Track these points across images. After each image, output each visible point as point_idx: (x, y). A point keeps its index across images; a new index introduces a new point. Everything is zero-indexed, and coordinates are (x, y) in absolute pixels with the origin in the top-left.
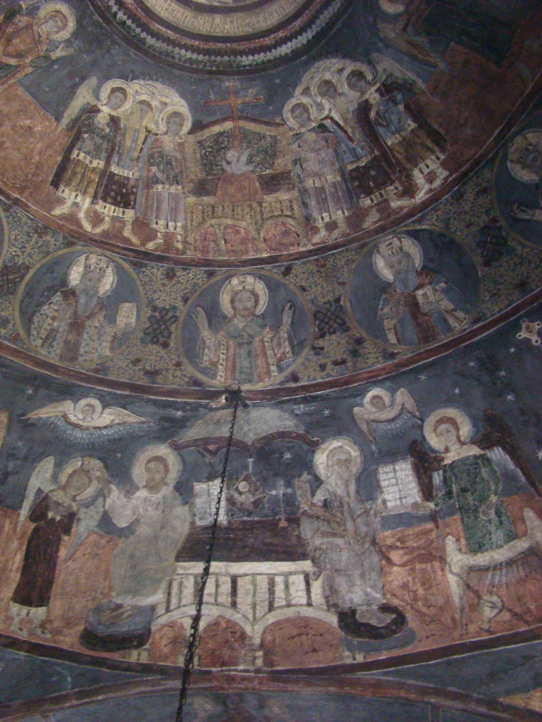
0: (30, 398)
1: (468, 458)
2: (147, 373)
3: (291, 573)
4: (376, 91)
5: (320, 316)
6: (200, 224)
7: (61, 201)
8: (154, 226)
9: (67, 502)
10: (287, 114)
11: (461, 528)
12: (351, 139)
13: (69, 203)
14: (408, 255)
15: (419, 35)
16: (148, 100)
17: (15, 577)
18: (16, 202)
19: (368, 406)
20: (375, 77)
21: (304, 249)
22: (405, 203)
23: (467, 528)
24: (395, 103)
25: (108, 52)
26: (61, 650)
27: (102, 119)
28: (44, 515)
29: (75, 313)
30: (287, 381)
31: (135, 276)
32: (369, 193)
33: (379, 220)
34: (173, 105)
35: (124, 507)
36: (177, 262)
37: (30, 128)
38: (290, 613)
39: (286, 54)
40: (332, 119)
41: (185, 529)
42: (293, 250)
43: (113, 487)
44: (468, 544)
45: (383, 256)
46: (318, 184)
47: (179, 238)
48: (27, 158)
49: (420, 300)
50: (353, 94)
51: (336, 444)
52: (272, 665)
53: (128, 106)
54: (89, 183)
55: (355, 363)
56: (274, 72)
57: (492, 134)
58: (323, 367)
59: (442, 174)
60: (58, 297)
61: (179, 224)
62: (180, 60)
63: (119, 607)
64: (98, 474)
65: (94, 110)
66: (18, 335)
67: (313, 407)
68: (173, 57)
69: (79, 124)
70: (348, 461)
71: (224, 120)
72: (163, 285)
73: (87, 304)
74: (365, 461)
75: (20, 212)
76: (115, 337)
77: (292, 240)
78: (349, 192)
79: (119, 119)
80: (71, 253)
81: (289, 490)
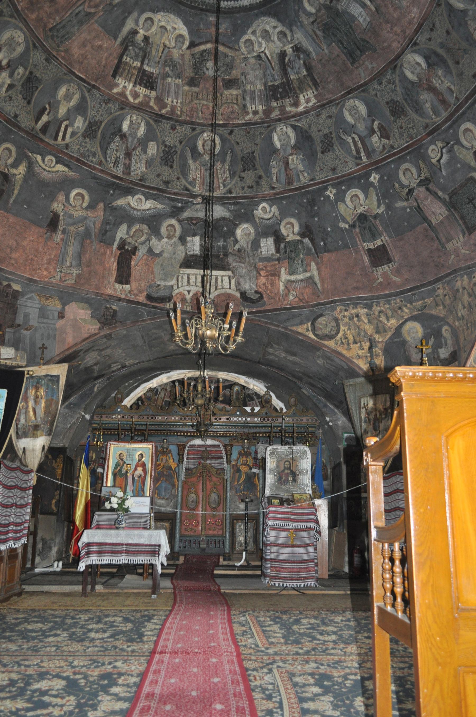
0: (112, 195)
1: (295, 240)
2: (164, 182)
3: (224, 276)
4: (291, 47)
5: (244, 159)
6: (190, 102)
7: (117, 85)
9: (133, 242)
10: (242, 45)
11: (287, 265)
12: (273, 68)
13: (121, 86)
14: (289, 137)
15: (319, 30)
16: (165, 25)
17: (115, 273)
18: (94, 86)
19: (260, 211)
20: (292, 40)
23: (290, 266)
26: (139, 302)
27: (139, 38)
28: (124, 248)
29: (127, 147)
30: (227, 193)
31: (155, 127)
32: (277, 100)
33: (279, 115)
34: (179, 29)
35: (157, 245)
36: (177, 121)
38: (223, 291)
39: (246, 6)
40: (265, 54)
41: (183, 255)
42: (235, 122)
43: (153, 237)
44: (289, 272)
45: (277, 134)
46: (252, 89)
47: (179, 108)
48: (99, 62)
49: (290, 160)
51: (245, 226)
52: (217, 311)
53: (154, 29)
55: (257, 189)
57: (340, 92)
58: (243, 188)
59: (314, 101)
60: (117, 139)
61: (179, 101)
63: (159, 285)
64: (147, 231)
65: (135, 32)
66: (101, 161)
70: (249, 234)
71: (207, 42)
72: (170, 133)
74: (256, 235)
75: (95, 91)
76: (147, 161)
77: (235, 116)
78: (267, 97)
79: (149, 37)
80: (123, 114)
81: (225, 243)
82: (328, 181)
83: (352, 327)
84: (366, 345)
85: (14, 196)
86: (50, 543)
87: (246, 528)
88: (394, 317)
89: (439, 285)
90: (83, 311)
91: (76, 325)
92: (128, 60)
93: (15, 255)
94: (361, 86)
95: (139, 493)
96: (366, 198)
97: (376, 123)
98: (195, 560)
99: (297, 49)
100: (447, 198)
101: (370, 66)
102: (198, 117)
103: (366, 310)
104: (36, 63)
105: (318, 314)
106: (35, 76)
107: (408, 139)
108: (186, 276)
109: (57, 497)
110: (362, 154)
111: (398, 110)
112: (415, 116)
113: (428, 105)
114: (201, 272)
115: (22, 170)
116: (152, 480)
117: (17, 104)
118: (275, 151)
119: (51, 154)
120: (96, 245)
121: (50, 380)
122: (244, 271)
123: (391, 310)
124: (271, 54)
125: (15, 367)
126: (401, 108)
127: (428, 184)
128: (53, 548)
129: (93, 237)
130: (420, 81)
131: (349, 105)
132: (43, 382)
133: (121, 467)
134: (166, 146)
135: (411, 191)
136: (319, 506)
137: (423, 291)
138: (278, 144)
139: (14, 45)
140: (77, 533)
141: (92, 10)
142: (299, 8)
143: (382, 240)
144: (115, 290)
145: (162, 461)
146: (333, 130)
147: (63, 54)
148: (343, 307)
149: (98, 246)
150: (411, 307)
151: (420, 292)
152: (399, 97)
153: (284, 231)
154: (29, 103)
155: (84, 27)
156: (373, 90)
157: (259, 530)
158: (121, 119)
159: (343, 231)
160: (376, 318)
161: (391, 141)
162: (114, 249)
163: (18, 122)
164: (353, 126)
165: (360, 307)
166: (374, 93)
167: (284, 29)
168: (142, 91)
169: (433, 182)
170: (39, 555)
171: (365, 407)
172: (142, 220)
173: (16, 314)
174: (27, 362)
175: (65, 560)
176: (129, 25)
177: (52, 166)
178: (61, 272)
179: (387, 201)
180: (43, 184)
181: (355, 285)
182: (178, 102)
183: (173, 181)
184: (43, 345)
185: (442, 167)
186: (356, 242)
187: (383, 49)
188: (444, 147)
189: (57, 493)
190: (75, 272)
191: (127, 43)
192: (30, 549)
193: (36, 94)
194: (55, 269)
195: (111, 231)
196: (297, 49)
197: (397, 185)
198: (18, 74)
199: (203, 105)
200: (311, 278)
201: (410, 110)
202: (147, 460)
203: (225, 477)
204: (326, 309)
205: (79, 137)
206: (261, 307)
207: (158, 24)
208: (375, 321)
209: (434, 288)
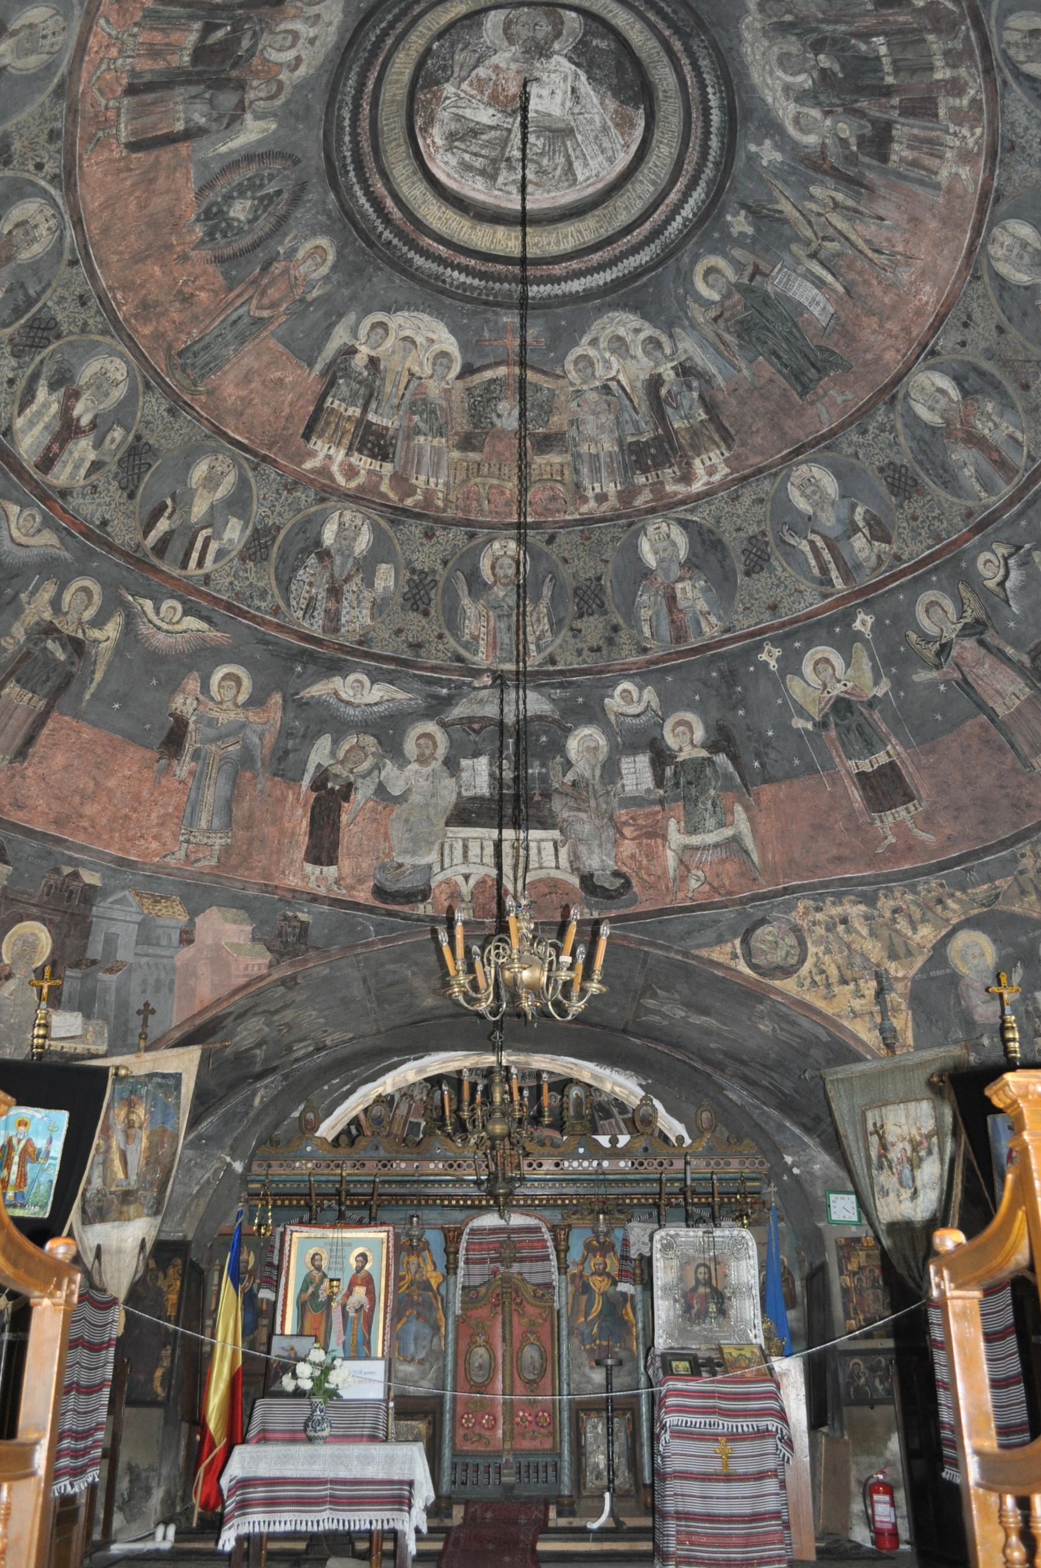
0: (299, 676)
2: (411, 646)
6: (464, 481)
8: (414, 481)
9: (345, 774)
10: (569, 366)
12: (634, 408)
13: (321, 456)
15: (730, 333)
17: (304, 841)
18: (265, 459)
19: (618, 699)
21: (570, 518)
22: (681, 489)
23: (687, 813)
24: (690, 388)
25: (370, 280)
27: (359, 361)
28: (324, 786)
29: (332, 576)
30: (545, 663)
31: (391, 533)
32: (645, 470)
33: (652, 501)
35: (397, 778)
36: (437, 520)
37: (281, 381)
38: (542, 874)
39: (577, 292)
40: (618, 382)
41: (454, 797)
43: (388, 762)
46: (593, 451)
47: (440, 495)
50: (646, 363)
51: (586, 731)
53: (389, 343)
54: (343, 434)
55: (609, 653)
56: (560, 310)
57: (780, 451)
58: (579, 652)
59: (723, 471)
60: (312, 560)
61: (441, 481)
62: (451, 284)
63: (400, 865)
64: (373, 749)
65: (352, 351)
66: (278, 607)
67: (567, 694)
68: (444, 282)
69: (334, 368)
70: (596, 749)
71: (497, 364)
72: (422, 544)
73: (343, 565)
74: (611, 751)
76: (374, 603)
77: (558, 506)
78: (625, 466)
79: (378, 359)
80: (324, 510)
81: (544, 770)
82: (761, 632)
83: (835, 947)
84: (870, 987)
85: (94, 684)
86: (147, 1478)
87: (610, 1433)
88: (928, 921)
89: (1024, 847)
90: (234, 927)
91: (218, 959)
92: (335, 406)
93: (89, 810)
94: (823, 437)
95: (359, 1350)
96: (848, 665)
97: (860, 510)
98: (489, 1515)
99: (685, 371)
100: (1026, 660)
101: (839, 399)
102: (482, 510)
103: (862, 908)
104: (149, 418)
105: (755, 918)
106: (147, 443)
107: (930, 542)
108: (460, 843)
109: (166, 1363)
110: (834, 574)
111: (906, 483)
112: (943, 495)
113: (968, 472)
114: (494, 834)
115: (112, 630)
116: (389, 1316)
117: (108, 499)
118: (646, 573)
119: (173, 597)
120: (264, 782)
121: (160, 1086)
122: (587, 827)
123: (919, 905)
124: (631, 382)
125: (83, 1057)
126: (912, 478)
127: (982, 633)
128: (155, 1491)
129: (259, 764)
130: (948, 425)
131: (800, 476)
132: (144, 1091)
133: (317, 1288)
134: (413, 571)
135: (945, 649)
136: (785, 1374)
137: (988, 862)
138: (650, 559)
139: (106, 385)
140: (211, 1450)
141: (265, 314)
142: (686, 293)
143: (888, 753)
144: (305, 877)
145: (408, 1270)
146: (767, 527)
147: (203, 398)
148: (811, 902)
149: (269, 783)
150: (964, 897)
151: (982, 864)
152: (906, 458)
153: (671, 741)
154: (131, 496)
155: (249, 346)
156: (850, 445)
157: (641, 1436)
158: (321, 520)
159: (801, 737)
160: (886, 925)
161: (895, 547)
162: (304, 789)
163: (109, 534)
164: (810, 518)
165: (850, 901)
166: (850, 451)
167: (657, 333)
168: (364, 463)
169: (993, 626)
170: (121, 1509)
171: (877, 1132)
172: (364, 726)
173: (87, 937)
174: (109, 1045)
175: (183, 1520)
176: (340, 337)
177: (175, 620)
178: (188, 842)
179: (894, 670)
180: (156, 658)
181: (834, 852)
182: (438, 484)
183: (430, 642)
184: (146, 1005)
185: (1010, 595)
186: (831, 758)
187: (865, 364)
188: (1011, 555)
189: (167, 1352)
190: (218, 841)
191: (335, 373)
192: (101, 1496)
193: (146, 479)
194: (175, 836)
195: (295, 750)
196: (685, 371)
197: (913, 637)
198: (113, 441)
199: (491, 487)
200: (736, 840)
201: (930, 483)
202: (377, 1267)
203: (556, 1305)
204: (771, 909)
205: (231, 560)
206: (627, 907)
207: (397, 334)
208: (886, 933)
209: (1014, 855)
